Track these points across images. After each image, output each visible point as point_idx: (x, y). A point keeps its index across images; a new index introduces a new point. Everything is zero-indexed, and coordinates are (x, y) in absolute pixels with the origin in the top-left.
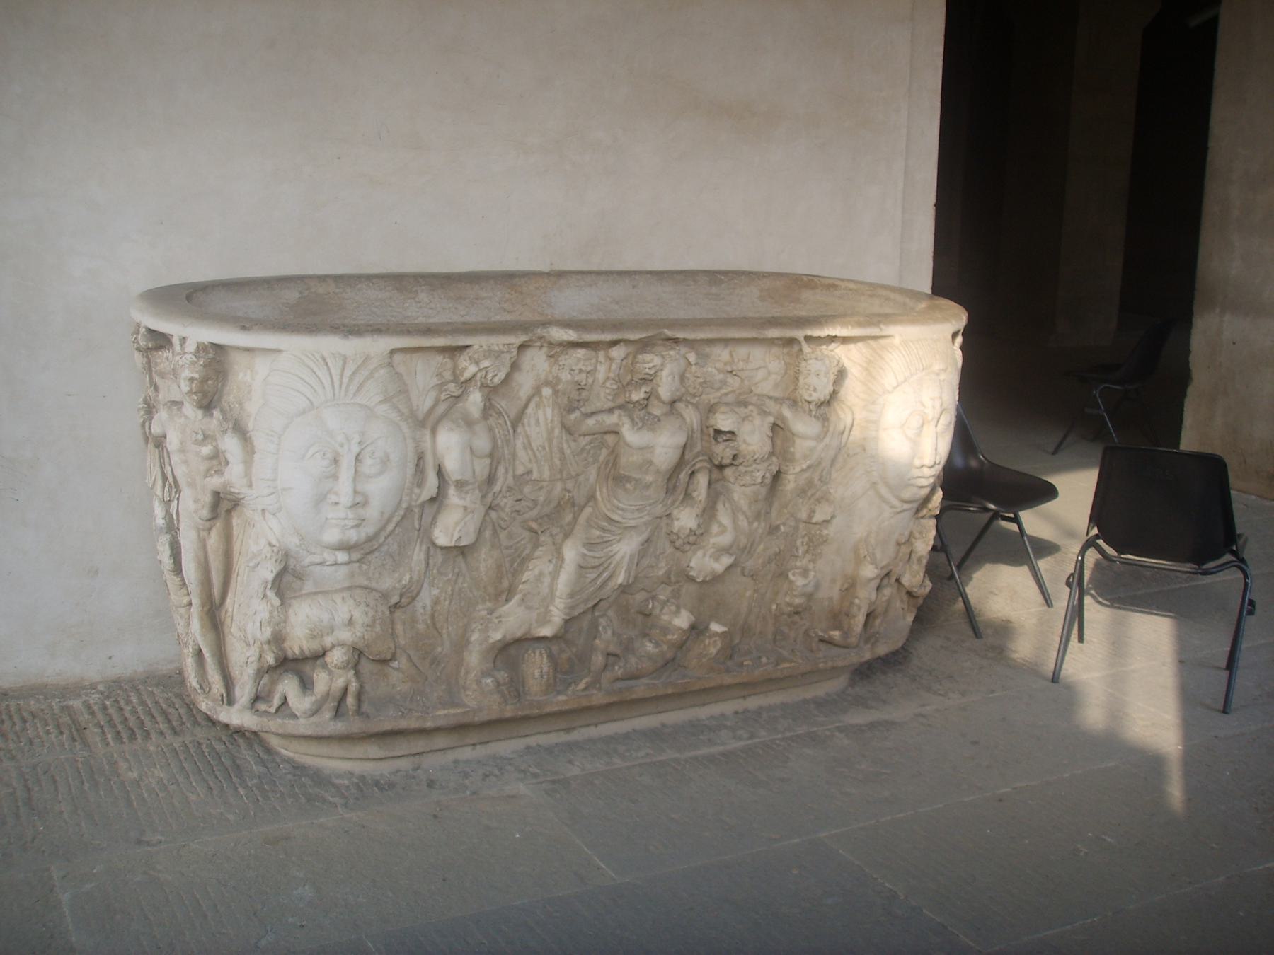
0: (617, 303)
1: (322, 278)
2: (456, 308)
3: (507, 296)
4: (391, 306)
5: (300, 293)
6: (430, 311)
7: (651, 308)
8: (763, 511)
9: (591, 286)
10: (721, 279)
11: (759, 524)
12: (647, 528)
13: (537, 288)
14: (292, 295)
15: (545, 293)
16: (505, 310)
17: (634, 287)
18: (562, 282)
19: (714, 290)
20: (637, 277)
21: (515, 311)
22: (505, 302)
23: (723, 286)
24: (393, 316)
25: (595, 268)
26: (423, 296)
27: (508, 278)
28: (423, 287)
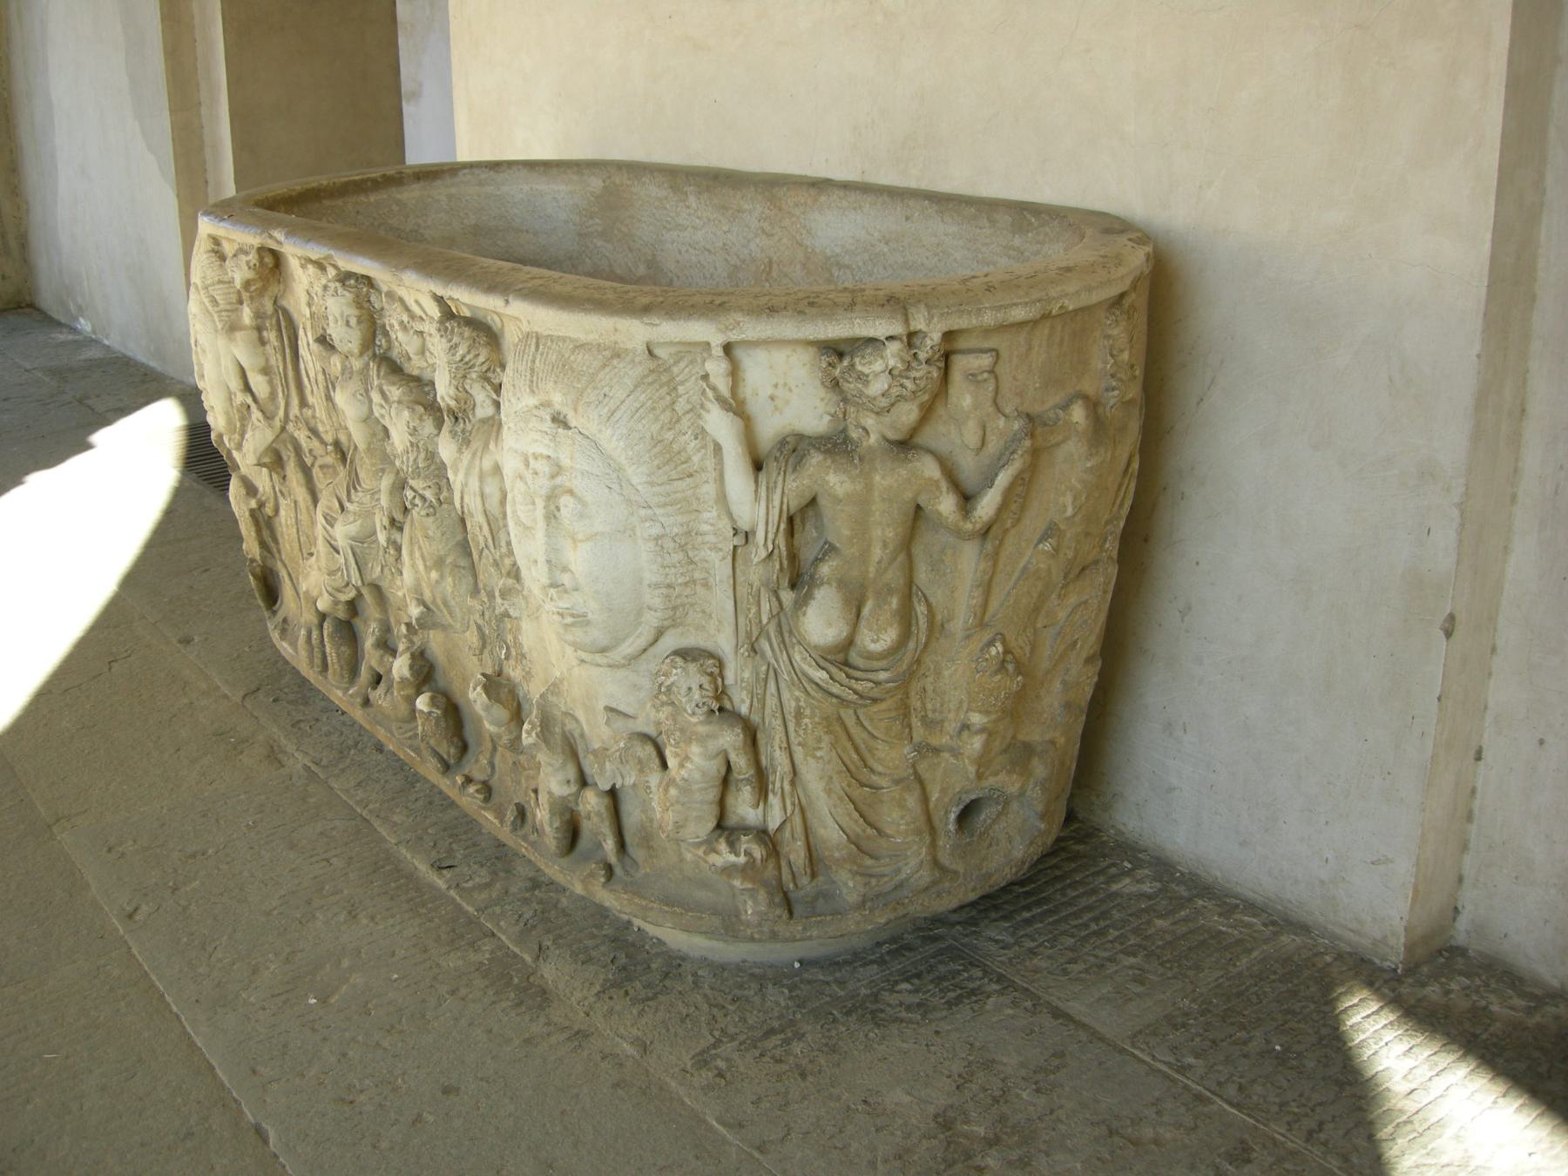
0: (887, 243)
1: (621, 166)
2: (720, 221)
3: (767, 211)
4: (666, 209)
5: (604, 181)
6: (697, 221)
7: (927, 258)
8: (449, 560)
9: (855, 209)
10: (1030, 224)
11: (442, 576)
12: (355, 521)
13: (796, 205)
14: (596, 183)
15: (803, 213)
16: (764, 231)
17: (907, 219)
18: (823, 198)
19: (1017, 241)
20: (912, 203)
21: (773, 235)
22: (765, 219)
23: (1030, 234)
24: (667, 221)
25: (913, 184)
26: (692, 200)
27: (770, 185)
28: (692, 188)
